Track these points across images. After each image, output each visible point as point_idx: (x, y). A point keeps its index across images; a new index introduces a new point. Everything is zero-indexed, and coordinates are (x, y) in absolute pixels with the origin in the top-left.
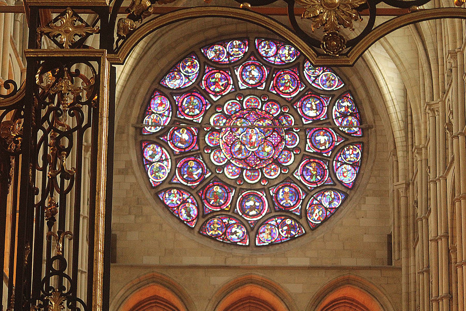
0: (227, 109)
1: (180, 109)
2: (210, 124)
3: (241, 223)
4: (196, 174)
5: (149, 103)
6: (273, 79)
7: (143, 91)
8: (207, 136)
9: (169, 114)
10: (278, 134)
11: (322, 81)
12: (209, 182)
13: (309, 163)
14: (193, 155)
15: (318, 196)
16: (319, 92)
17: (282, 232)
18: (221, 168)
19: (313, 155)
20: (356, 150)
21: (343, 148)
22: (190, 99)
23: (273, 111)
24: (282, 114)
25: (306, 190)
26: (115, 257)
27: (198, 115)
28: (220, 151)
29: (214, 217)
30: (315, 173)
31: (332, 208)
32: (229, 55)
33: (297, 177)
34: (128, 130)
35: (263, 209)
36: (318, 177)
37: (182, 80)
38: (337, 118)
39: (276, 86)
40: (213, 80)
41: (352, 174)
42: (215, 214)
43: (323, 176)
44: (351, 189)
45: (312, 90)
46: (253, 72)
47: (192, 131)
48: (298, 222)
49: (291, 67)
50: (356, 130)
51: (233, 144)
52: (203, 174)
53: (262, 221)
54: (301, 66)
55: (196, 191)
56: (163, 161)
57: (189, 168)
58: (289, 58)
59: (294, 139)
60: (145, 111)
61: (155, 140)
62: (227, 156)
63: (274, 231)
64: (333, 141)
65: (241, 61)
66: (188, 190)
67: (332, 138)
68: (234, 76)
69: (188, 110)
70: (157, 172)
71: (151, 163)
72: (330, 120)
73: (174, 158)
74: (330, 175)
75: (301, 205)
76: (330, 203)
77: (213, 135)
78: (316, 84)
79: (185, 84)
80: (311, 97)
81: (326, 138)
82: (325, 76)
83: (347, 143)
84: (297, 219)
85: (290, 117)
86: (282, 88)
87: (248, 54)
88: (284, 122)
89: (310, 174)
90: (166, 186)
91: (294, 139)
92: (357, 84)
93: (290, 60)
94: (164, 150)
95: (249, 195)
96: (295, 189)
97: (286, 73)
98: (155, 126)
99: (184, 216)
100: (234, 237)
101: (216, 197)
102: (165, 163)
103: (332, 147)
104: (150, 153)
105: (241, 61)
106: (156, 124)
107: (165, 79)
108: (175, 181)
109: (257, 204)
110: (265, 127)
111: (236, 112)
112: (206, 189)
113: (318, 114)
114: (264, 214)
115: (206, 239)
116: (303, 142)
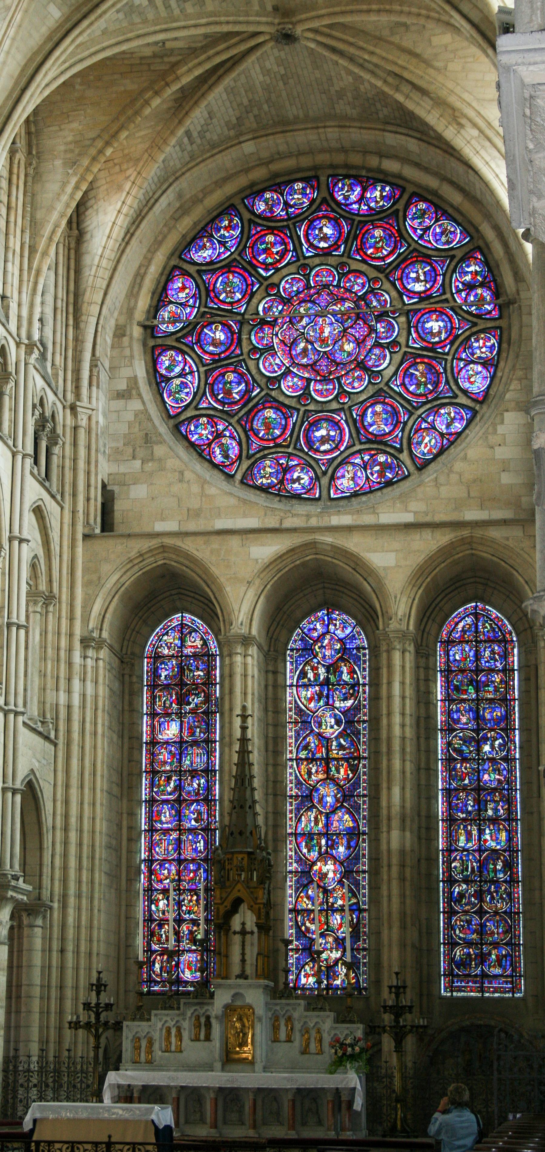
0: (284, 289)
1: (212, 294)
2: (258, 313)
3: (307, 466)
4: (237, 391)
5: (165, 289)
6: (355, 238)
7: (154, 270)
8: (253, 333)
9: (195, 303)
10: (365, 323)
11: (435, 235)
12: (257, 404)
13: (414, 365)
14: (231, 364)
15: (428, 416)
16: (430, 252)
17: (372, 474)
18: (276, 380)
19: (420, 352)
20: (489, 339)
21: (468, 338)
22: (228, 278)
23: (356, 288)
24: (371, 291)
25: (410, 408)
26: (112, 524)
27: (239, 301)
28: (274, 355)
29: (265, 457)
30: (423, 380)
31: (451, 434)
32: (287, 205)
33: (396, 388)
34: (131, 329)
35: (341, 441)
36: (429, 386)
37: (215, 249)
38: (459, 291)
39: (362, 249)
40: (263, 246)
41: (484, 378)
42: (266, 452)
43: (436, 384)
44: (481, 403)
45: (419, 252)
46: (326, 230)
47: (230, 327)
48: (397, 458)
49: (385, 217)
50: (489, 308)
51: (295, 343)
52: (248, 391)
53: (339, 459)
54: (401, 214)
55: (236, 418)
56: (186, 374)
57: (225, 384)
58: (381, 203)
59: (389, 330)
60: (159, 300)
61: (175, 344)
62: (285, 362)
63: (359, 474)
64: (452, 328)
65: (307, 214)
66: (225, 417)
67: (451, 323)
68: (295, 238)
69: (224, 295)
70: (178, 393)
71: (168, 380)
72: (448, 296)
73: (202, 369)
74: (447, 382)
75: (403, 430)
76: (448, 426)
77: (262, 330)
78: (425, 241)
79: (219, 255)
80: (417, 261)
81: (441, 324)
82: (440, 226)
83: (475, 329)
84: (396, 454)
85: (383, 295)
86: (370, 251)
87: (318, 202)
88: (375, 304)
89: (415, 381)
90: (190, 413)
91: (390, 328)
92: (490, 234)
93: (384, 206)
94: (188, 359)
95: (321, 419)
96: (392, 406)
97: (378, 227)
98: (174, 323)
99: (219, 458)
100: (296, 485)
101: (268, 426)
102: (189, 377)
103: (451, 338)
104: (167, 363)
105: (307, 214)
106: (175, 319)
107: (189, 251)
108: (205, 405)
109: (332, 433)
110: (343, 314)
111: (298, 292)
112: (253, 414)
113: (428, 286)
114: (342, 449)
115: (252, 491)
116: (404, 333)
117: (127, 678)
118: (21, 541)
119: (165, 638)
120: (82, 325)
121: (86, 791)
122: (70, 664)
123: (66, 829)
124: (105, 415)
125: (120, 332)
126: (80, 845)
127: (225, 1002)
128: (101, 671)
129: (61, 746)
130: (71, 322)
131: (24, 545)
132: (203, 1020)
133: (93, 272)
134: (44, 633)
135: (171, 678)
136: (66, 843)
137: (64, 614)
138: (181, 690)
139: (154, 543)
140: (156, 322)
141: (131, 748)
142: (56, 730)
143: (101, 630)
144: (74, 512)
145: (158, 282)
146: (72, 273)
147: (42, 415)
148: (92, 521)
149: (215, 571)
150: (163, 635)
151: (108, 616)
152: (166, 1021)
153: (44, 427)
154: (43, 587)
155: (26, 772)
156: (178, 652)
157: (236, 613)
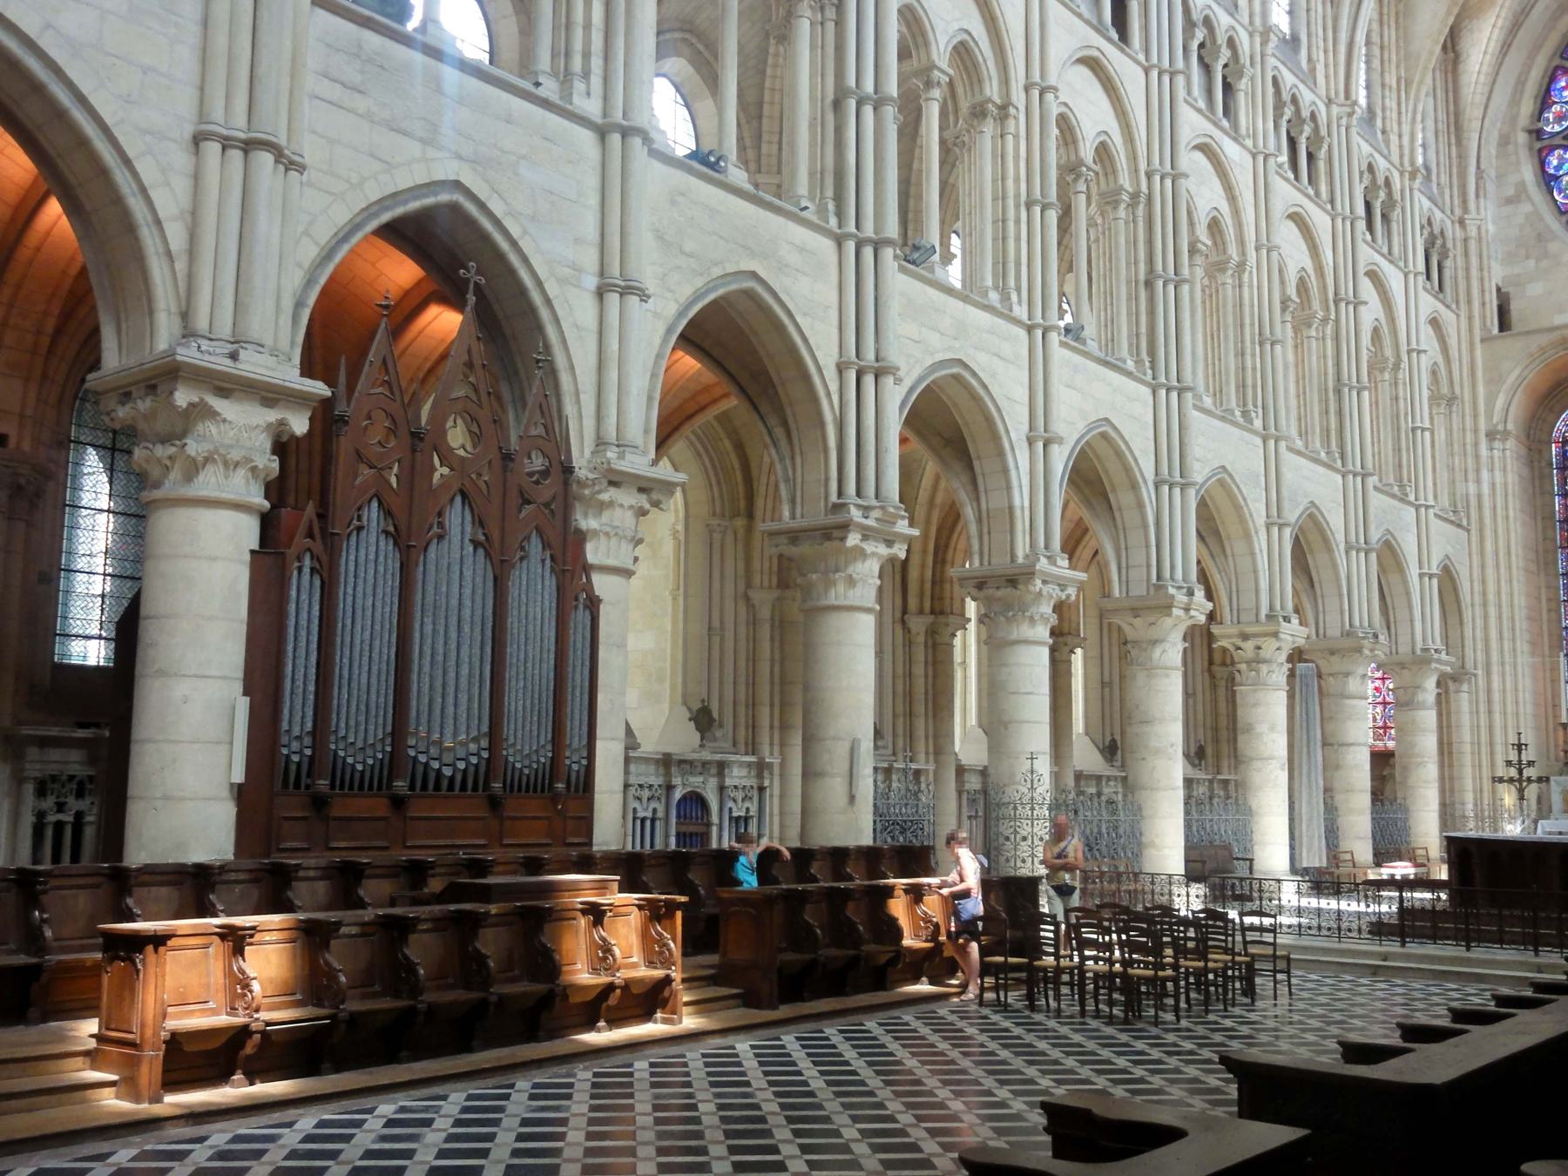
5: (1548, 91)
104: (1555, 162)
117: (1536, 463)
118: (1419, 352)
120: (1465, 142)
121: (1502, 570)
122: (1477, 456)
123: (1485, 605)
124: (1494, 222)
125: (1504, 141)
126: (1500, 617)
128: (1509, 461)
129: (1473, 532)
130: (1453, 141)
131: (1423, 356)
133: (1472, 90)
134: (1450, 431)
136: (1486, 617)
137: (1467, 411)
139: (1556, 335)
140: (1540, 125)
141: (1544, 529)
143: (1506, 422)
144: (1470, 318)
145: (1541, 85)
146: (1451, 95)
147: (1432, 234)
148: (1489, 323)
151: (1513, 409)
153: (1433, 244)
154: (1445, 390)
155: (1441, 557)
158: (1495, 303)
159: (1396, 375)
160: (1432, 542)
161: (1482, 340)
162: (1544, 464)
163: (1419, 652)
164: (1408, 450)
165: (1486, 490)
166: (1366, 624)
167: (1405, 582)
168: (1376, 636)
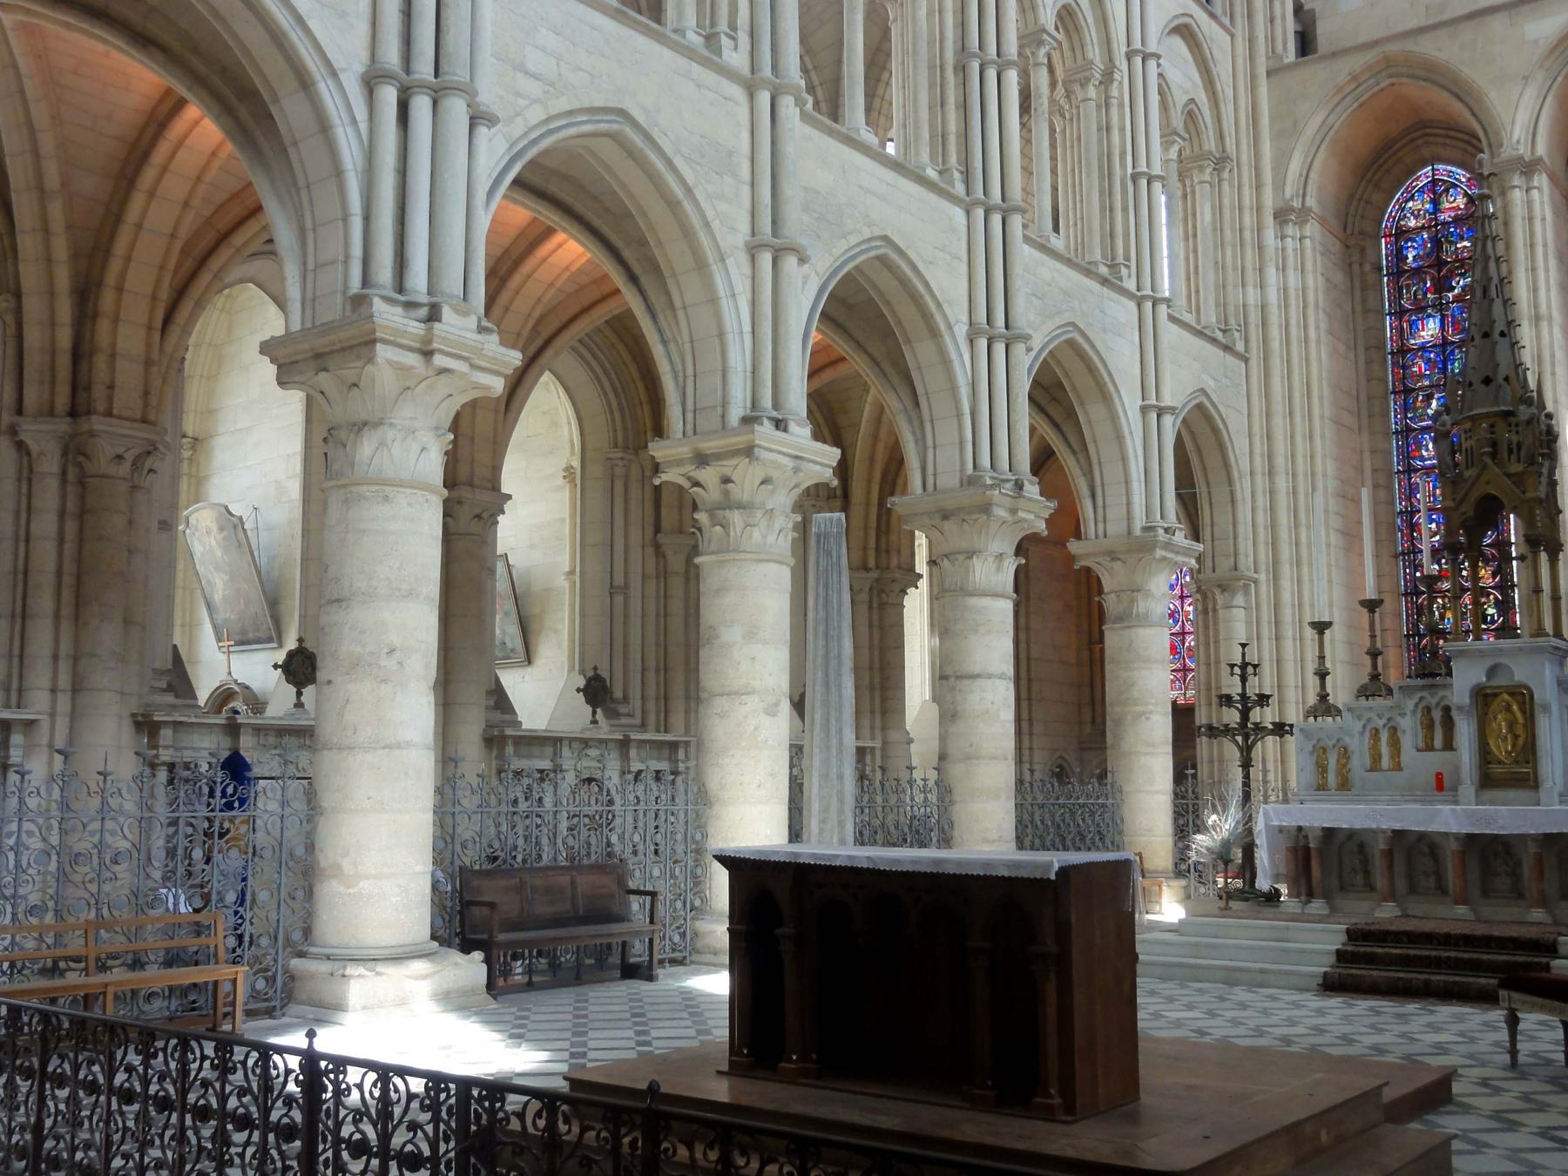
117: (1356, 267)
119: (1410, 204)
127: (1474, 681)
128: (1309, 252)
129: (1254, 362)
132: (1437, 715)
135: (1422, 258)
138: (1439, 272)
139: (1369, 57)
141: (1368, 363)
142: (1247, 341)
143: (1304, 196)
144: (1251, 40)
148: (1279, 48)
149: (1469, 73)
150: (1407, 201)
152: (1369, 720)
156: (1431, 220)
157: (1508, 129)
158: (1291, 26)
159: (1106, 91)
160: (1165, 354)
161: (1269, 73)
162: (1367, 267)
163: (1137, 532)
164: (1125, 209)
165: (1273, 296)
166: (1004, 463)
167: (1114, 418)
168: (1019, 486)
